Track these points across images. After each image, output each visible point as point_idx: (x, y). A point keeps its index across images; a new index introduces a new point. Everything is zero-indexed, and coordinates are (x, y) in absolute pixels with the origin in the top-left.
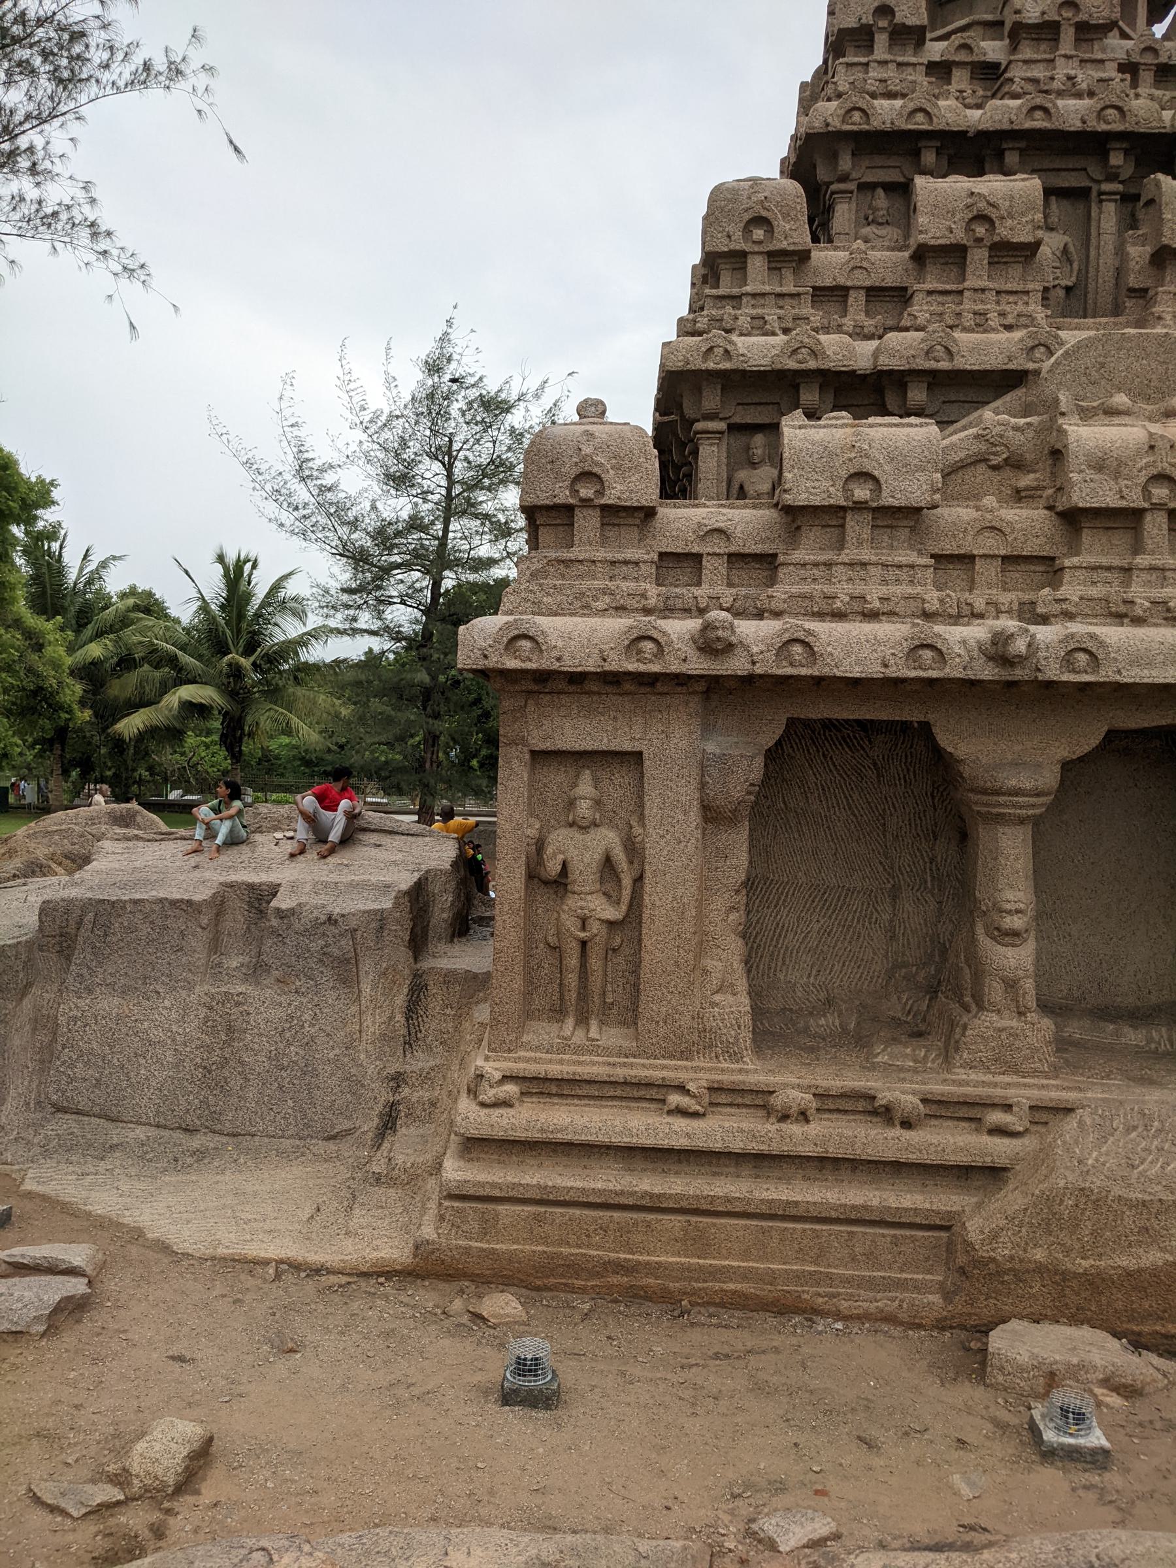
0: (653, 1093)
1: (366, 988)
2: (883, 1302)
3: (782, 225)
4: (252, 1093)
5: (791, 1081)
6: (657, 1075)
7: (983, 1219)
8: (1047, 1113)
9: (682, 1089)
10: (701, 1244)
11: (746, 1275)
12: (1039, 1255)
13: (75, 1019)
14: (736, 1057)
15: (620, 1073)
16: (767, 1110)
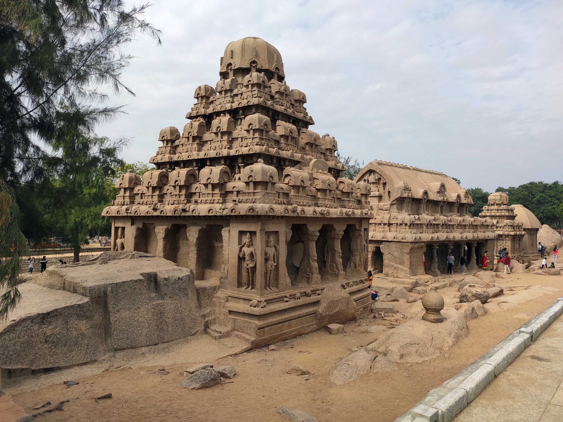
0: (282, 299)
1: (190, 295)
2: (310, 329)
3: (269, 126)
4: (170, 329)
5: (297, 292)
6: (283, 295)
7: (321, 309)
8: (323, 289)
9: (286, 297)
10: (290, 326)
11: (295, 330)
12: (327, 313)
13: (116, 321)
14: (290, 289)
15: (279, 296)
16: (295, 298)
